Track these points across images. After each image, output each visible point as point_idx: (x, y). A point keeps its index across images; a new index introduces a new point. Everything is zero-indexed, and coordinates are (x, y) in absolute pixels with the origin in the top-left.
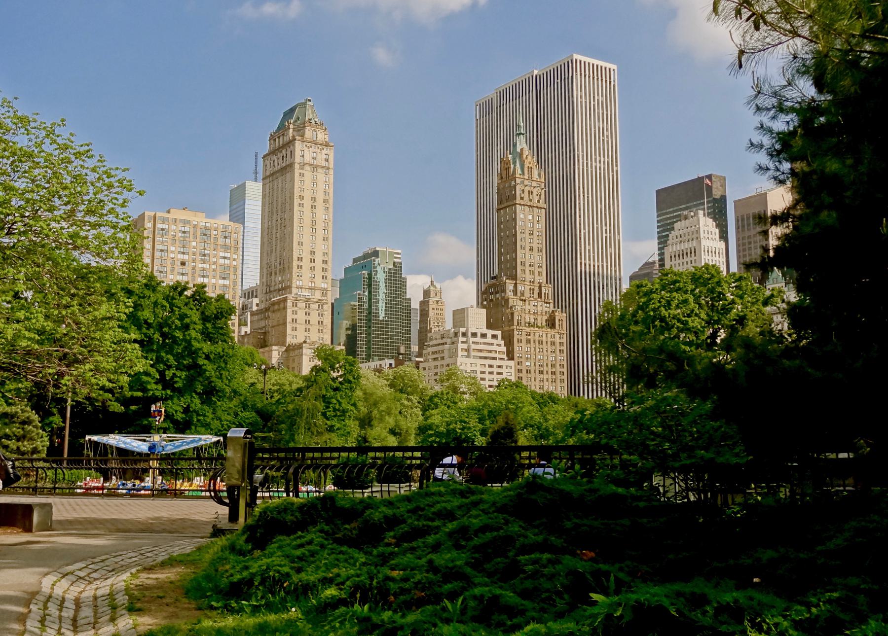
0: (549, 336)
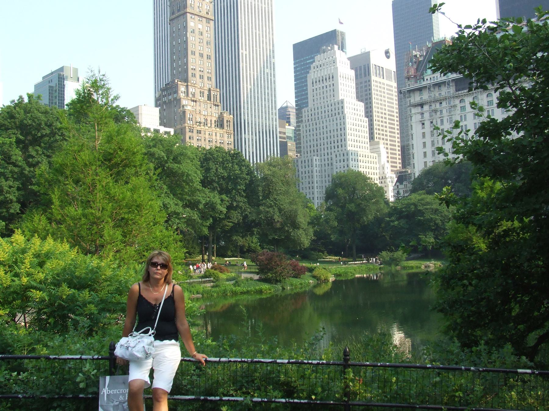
0: (218, 134)
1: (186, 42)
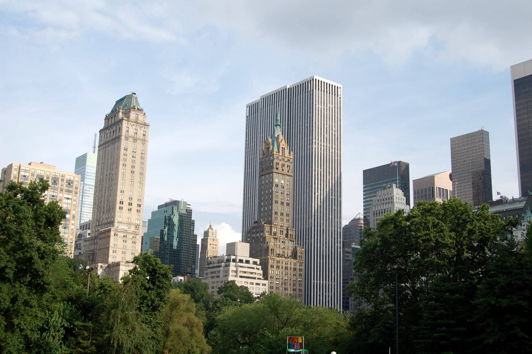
0: (292, 264)
1: (272, 194)
